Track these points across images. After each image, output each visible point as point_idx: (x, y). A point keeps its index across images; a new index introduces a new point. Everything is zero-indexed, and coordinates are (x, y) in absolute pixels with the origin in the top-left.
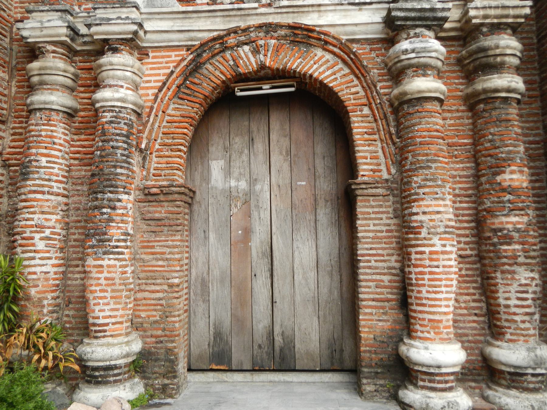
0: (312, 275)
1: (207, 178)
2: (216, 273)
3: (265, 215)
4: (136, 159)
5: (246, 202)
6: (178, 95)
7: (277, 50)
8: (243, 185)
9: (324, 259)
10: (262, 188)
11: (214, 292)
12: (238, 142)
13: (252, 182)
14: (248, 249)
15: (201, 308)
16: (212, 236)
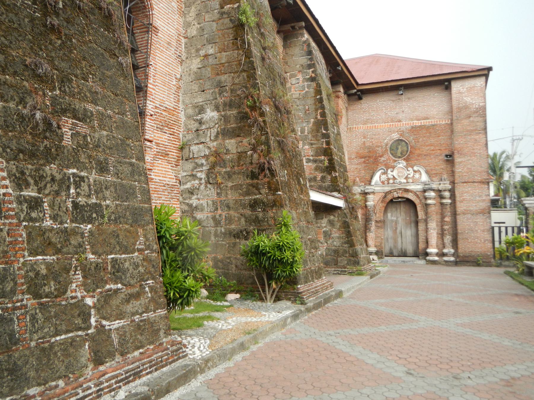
0: (410, 237)
1: (387, 217)
2: (390, 237)
3: (400, 225)
4: (374, 215)
5: (396, 222)
6: (382, 202)
7: (402, 193)
8: (395, 219)
9: (413, 234)
10: (400, 220)
11: (390, 240)
12: (394, 209)
13: (397, 218)
14: (396, 232)
15: (387, 244)
16: (389, 229)
